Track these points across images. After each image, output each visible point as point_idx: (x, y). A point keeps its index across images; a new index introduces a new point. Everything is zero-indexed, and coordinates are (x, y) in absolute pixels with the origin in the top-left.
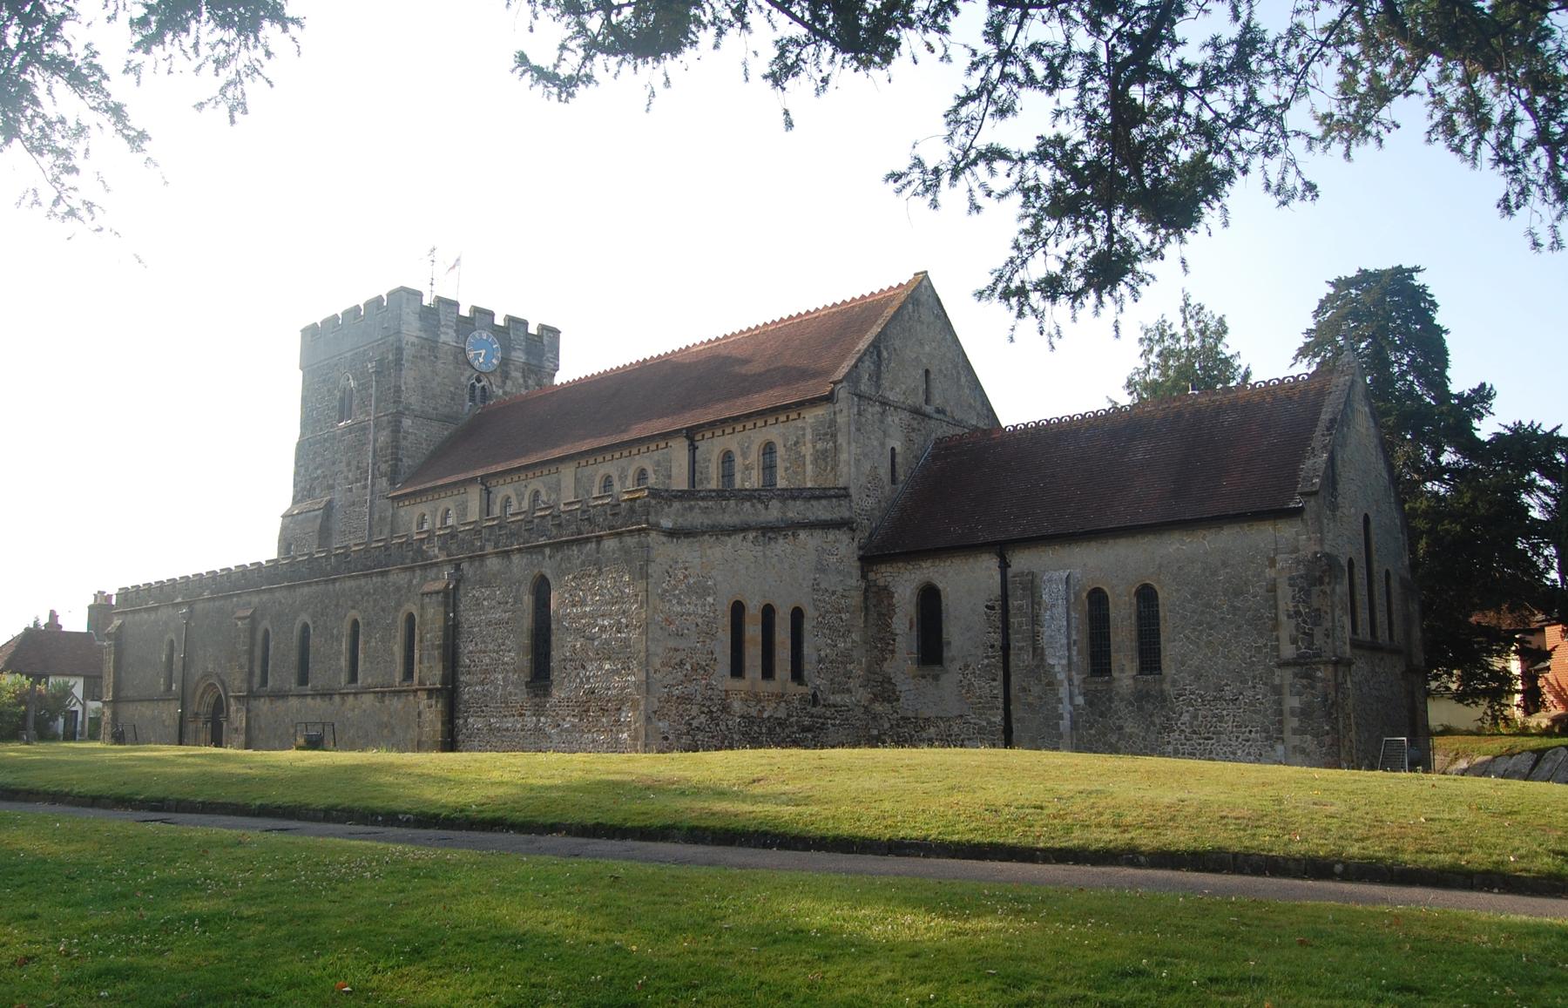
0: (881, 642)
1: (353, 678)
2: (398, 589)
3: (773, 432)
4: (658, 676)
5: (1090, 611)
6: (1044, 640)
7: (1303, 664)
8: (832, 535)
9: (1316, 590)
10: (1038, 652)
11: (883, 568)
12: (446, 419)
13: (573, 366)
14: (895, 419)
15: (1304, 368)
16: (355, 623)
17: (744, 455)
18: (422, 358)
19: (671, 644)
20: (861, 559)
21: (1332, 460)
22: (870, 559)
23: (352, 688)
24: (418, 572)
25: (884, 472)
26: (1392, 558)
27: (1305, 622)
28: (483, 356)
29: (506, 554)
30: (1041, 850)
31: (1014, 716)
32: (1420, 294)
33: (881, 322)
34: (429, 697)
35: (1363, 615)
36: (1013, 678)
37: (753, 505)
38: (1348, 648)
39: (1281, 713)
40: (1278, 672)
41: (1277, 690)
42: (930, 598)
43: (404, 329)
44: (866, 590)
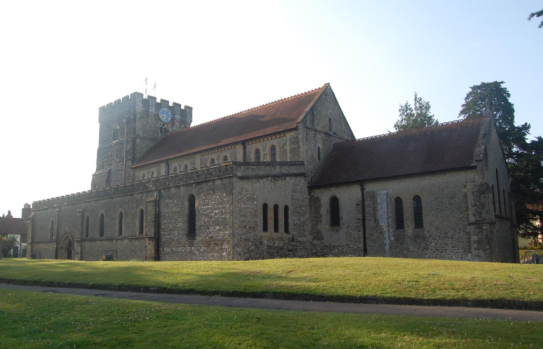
0: (316, 218)
1: (121, 233)
2: (137, 200)
3: (275, 142)
4: (237, 231)
5: (396, 205)
6: (379, 216)
7: (478, 224)
8: (298, 179)
9: (482, 196)
10: (376, 221)
11: (317, 191)
12: (152, 140)
13: (197, 120)
14: (319, 137)
15: (462, 118)
16: (121, 213)
17: (264, 150)
18: (143, 117)
19: (242, 219)
20: (308, 187)
21: (486, 148)
22: (311, 188)
23: (120, 237)
24: (145, 194)
25: (316, 156)
26: (505, 184)
27: (478, 208)
28: (165, 117)
29: (178, 187)
30: (426, 300)
31: (367, 245)
32: (504, 90)
33: (314, 101)
34: (150, 240)
35: (497, 205)
36: (367, 230)
37: (270, 168)
38: (494, 217)
39: (470, 242)
40: (468, 227)
41: (468, 234)
42: (334, 202)
43: (137, 107)
44: (310, 199)
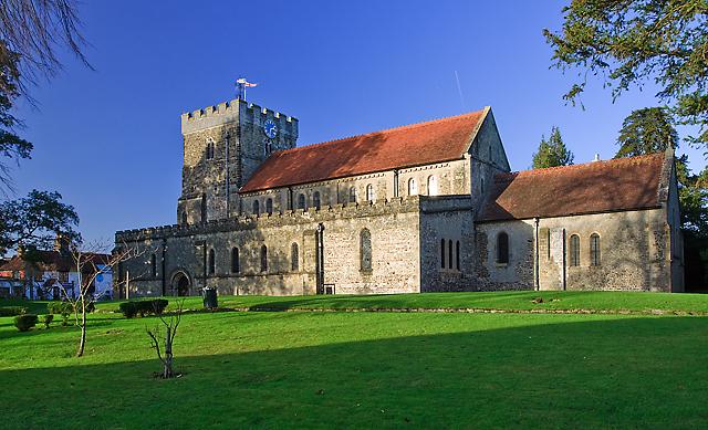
12: (257, 158)
22: (477, 223)
